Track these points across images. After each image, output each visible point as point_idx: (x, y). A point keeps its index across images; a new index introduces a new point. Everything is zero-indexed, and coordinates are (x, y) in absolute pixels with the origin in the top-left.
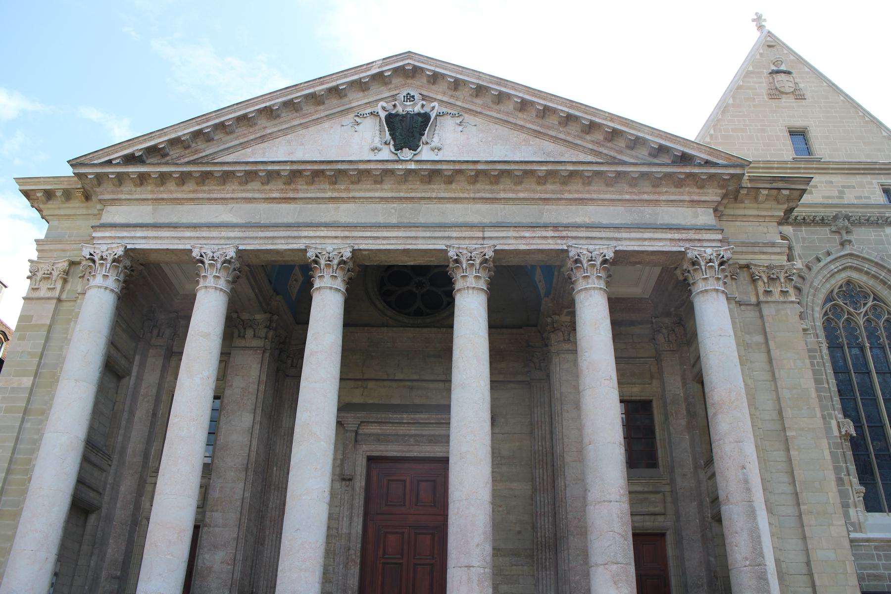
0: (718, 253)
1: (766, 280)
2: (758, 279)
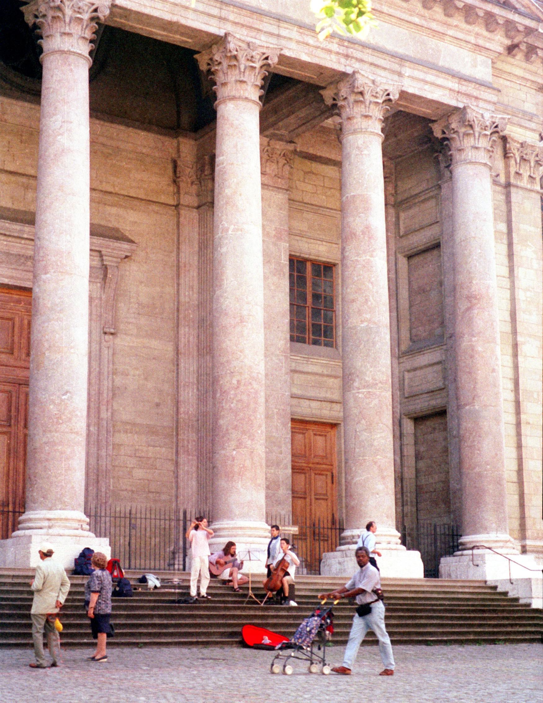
0: (494, 120)
1: (518, 161)
2: (511, 157)
